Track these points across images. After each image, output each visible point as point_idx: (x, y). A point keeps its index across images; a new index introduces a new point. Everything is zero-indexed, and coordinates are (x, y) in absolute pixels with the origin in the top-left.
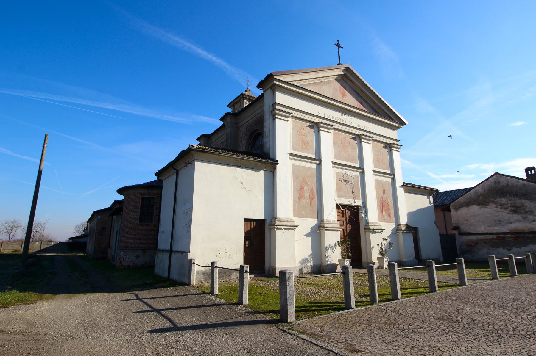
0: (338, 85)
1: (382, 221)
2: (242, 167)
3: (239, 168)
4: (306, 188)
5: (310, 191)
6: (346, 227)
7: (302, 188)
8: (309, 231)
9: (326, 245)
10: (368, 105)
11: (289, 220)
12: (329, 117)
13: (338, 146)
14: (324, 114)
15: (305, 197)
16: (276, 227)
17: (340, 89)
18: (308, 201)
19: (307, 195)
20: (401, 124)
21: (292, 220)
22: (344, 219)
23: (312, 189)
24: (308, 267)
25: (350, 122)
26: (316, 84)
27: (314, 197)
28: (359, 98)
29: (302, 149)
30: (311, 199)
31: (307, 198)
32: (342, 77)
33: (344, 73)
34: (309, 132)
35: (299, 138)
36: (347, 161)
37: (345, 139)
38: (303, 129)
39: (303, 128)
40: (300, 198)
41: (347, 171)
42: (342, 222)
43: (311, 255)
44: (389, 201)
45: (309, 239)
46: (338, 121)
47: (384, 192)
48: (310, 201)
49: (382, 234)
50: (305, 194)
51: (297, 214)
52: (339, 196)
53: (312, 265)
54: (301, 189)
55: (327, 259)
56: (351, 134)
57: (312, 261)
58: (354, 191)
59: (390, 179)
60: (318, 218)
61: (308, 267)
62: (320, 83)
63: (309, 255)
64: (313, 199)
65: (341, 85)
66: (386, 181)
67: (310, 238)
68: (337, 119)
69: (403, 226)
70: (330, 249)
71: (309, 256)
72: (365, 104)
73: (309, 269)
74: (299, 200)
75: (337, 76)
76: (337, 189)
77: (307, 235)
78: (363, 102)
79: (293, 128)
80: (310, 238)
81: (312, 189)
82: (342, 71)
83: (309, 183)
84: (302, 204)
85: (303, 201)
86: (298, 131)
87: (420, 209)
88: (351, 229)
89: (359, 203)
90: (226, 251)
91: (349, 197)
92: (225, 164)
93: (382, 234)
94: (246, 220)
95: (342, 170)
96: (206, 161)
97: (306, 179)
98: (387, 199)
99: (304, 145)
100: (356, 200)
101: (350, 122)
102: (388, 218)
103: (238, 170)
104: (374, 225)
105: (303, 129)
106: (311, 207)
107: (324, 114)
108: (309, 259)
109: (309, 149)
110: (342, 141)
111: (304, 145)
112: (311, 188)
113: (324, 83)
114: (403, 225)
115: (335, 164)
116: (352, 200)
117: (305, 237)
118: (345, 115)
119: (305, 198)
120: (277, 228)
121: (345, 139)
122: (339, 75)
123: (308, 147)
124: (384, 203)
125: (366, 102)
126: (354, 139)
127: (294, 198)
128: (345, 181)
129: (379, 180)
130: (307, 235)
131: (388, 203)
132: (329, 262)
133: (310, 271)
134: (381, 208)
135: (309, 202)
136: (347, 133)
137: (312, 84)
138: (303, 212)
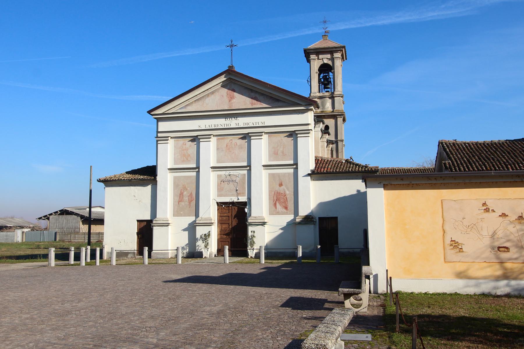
0: (226, 90)
1: (274, 213)
2: (135, 186)
3: (133, 186)
4: (185, 193)
5: (190, 196)
6: (232, 221)
7: (181, 194)
8: (186, 226)
9: (197, 237)
10: (265, 97)
11: (164, 220)
12: (211, 126)
13: (222, 150)
14: (205, 125)
15: (184, 200)
16: (154, 225)
17: (228, 94)
18: (187, 204)
19: (186, 199)
20: (309, 105)
21: (167, 220)
22: (230, 214)
23: (191, 193)
24: (184, 253)
25: (236, 124)
26: (198, 100)
27: (192, 200)
28: (253, 94)
29: (183, 162)
30: (190, 202)
31: (186, 201)
32: (230, 80)
33: (226, 79)
34: (190, 146)
35: (181, 153)
36: (234, 162)
37: (231, 142)
38: (185, 145)
39: (184, 144)
40: (179, 202)
41: (230, 171)
42: (228, 217)
43: (187, 244)
44: (287, 192)
45: (186, 233)
46: (221, 127)
47: (281, 185)
48: (189, 203)
49: (265, 226)
50: (184, 198)
51: (177, 213)
52: (219, 195)
53: (187, 252)
54: (180, 194)
55: (197, 248)
56: (238, 135)
57: (188, 249)
58: (237, 189)
59: (293, 169)
60: (195, 216)
61: (184, 253)
62: (203, 97)
63: (185, 244)
64: (192, 201)
65: (229, 89)
66: (286, 173)
67: (187, 232)
68: (220, 125)
69: (300, 218)
70: (200, 240)
71: (185, 245)
72: (261, 98)
73: (184, 255)
74: (178, 203)
75: (222, 83)
76: (217, 189)
77: (184, 230)
78: (257, 96)
79: (175, 147)
80: (187, 232)
81: (191, 193)
82: (224, 78)
83: (189, 189)
84: (181, 206)
85: (183, 203)
86: (179, 148)
87: (345, 197)
88: (237, 223)
89: (243, 199)
90: (125, 241)
91: (233, 195)
92: (123, 186)
93: (265, 226)
94: (138, 221)
95: (225, 172)
96: (112, 186)
97: (185, 186)
98: (285, 192)
99: (185, 158)
100: (239, 198)
101: (236, 124)
102: (285, 210)
103: (132, 188)
104: (255, 218)
105: (185, 145)
106: (189, 208)
107: (205, 125)
108: (185, 247)
109: (190, 160)
110: (228, 145)
111: (185, 157)
112: (190, 192)
113: (208, 95)
114: (301, 216)
115: (213, 169)
116: (235, 197)
117: (183, 231)
118: (231, 119)
119: (184, 201)
120: (155, 226)
121: (231, 142)
122: (222, 82)
123: (189, 159)
124: (279, 195)
125: (263, 94)
126: (242, 138)
127: (174, 202)
128: (229, 181)
129: (274, 174)
130: (184, 230)
131: (285, 195)
132: (199, 250)
133: (185, 256)
134: (273, 201)
135: (188, 204)
136: (234, 135)
137: (194, 102)
138: (182, 213)
